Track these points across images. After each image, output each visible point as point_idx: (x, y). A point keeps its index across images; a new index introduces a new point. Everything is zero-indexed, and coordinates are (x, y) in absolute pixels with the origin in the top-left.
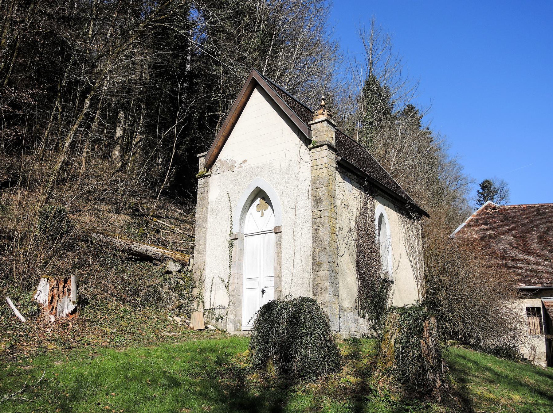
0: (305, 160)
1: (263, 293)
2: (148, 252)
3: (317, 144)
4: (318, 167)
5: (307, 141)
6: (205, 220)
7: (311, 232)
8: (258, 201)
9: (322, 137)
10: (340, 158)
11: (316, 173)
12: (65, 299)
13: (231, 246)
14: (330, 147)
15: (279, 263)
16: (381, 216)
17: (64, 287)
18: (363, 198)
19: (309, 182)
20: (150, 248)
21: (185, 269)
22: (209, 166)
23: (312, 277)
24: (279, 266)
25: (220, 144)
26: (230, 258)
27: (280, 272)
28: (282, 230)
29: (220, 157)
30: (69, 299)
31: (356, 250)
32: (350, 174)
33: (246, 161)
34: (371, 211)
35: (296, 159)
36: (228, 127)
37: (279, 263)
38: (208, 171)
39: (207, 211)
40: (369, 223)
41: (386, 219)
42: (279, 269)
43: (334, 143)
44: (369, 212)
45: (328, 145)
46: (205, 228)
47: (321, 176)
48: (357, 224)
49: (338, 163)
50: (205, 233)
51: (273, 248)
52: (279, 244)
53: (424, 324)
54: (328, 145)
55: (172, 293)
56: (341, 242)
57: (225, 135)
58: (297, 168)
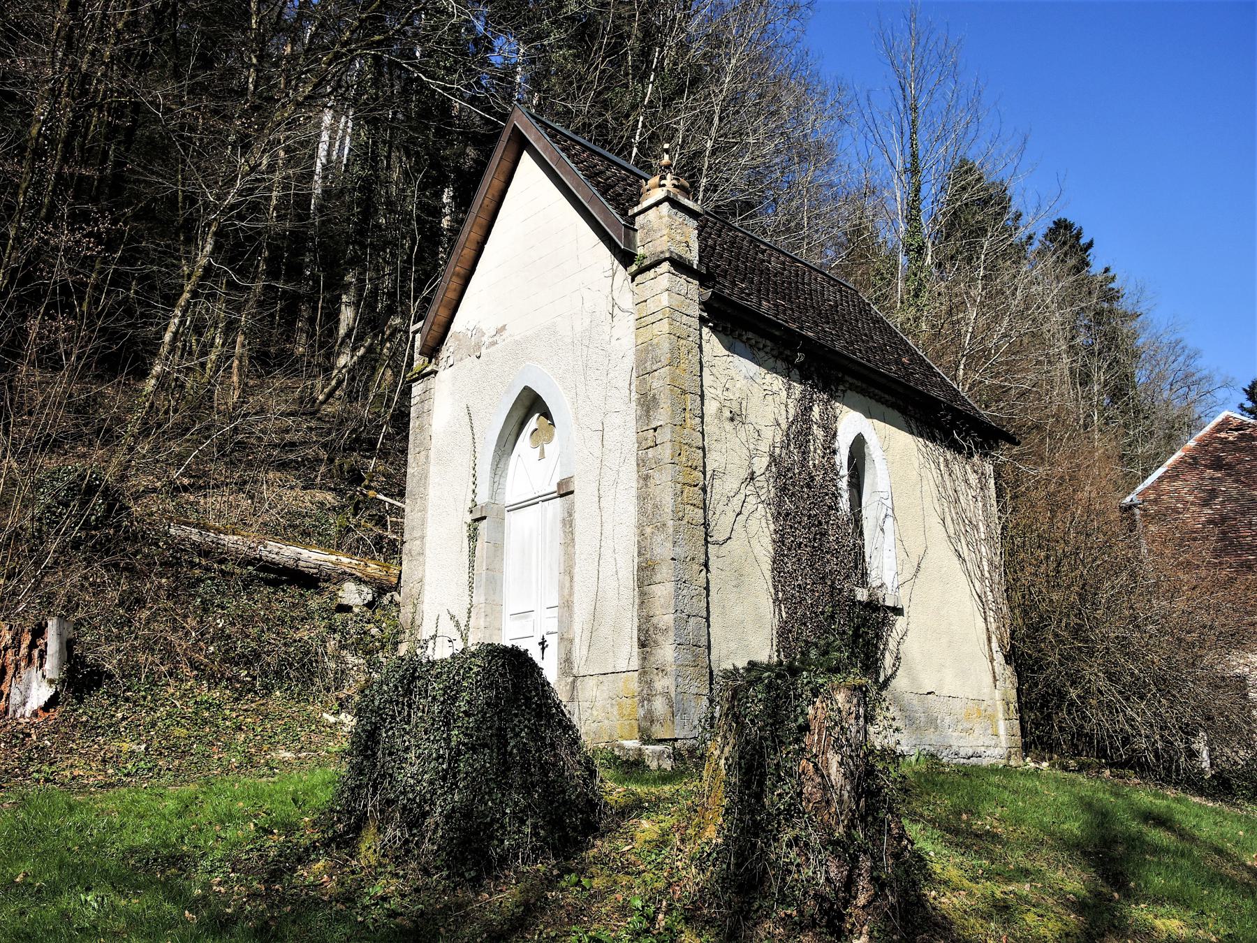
0: (622, 307)
1: (543, 649)
2: (301, 563)
3: (647, 262)
4: (650, 319)
5: (625, 257)
6: (424, 477)
7: (635, 485)
8: (533, 423)
9: (658, 242)
10: (709, 292)
11: (646, 334)
12: (34, 674)
13: (473, 537)
14: (680, 265)
15: (569, 572)
16: (858, 445)
17: (32, 646)
18: (798, 395)
19: (630, 361)
20: (305, 554)
21: (386, 600)
22: (433, 351)
23: (637, 601)
24: (567, 578)
25: (452, 295)
26: (471, 566)
27: (571, 594)
28: (576, 486)
29: (455, 327)
30: (40, 673)
31: (772, 527)
32: (750, 335)
33: (504, 328)
34: (825, 428)
35: (605, 306)
36: (468, 253)
37: (569, 572)
38: (430, 362)
39: (427, 457)
40: (815, 458)
41: (874, 448)
42: (568, 585)
43: (693, 257)
44: (818, 432)
45: (672, 261)
46: (424, 497)
47: (655, 341)
48: (774, 460)
49: (705, 305)
50: (424, 510)
51: (556, 534)
52: (568, 522)
53: (810, 710)
54: (672, 261)
55: (350, 659)
56: (720, 507)
57: (462, 272)
58: (607, 328)
